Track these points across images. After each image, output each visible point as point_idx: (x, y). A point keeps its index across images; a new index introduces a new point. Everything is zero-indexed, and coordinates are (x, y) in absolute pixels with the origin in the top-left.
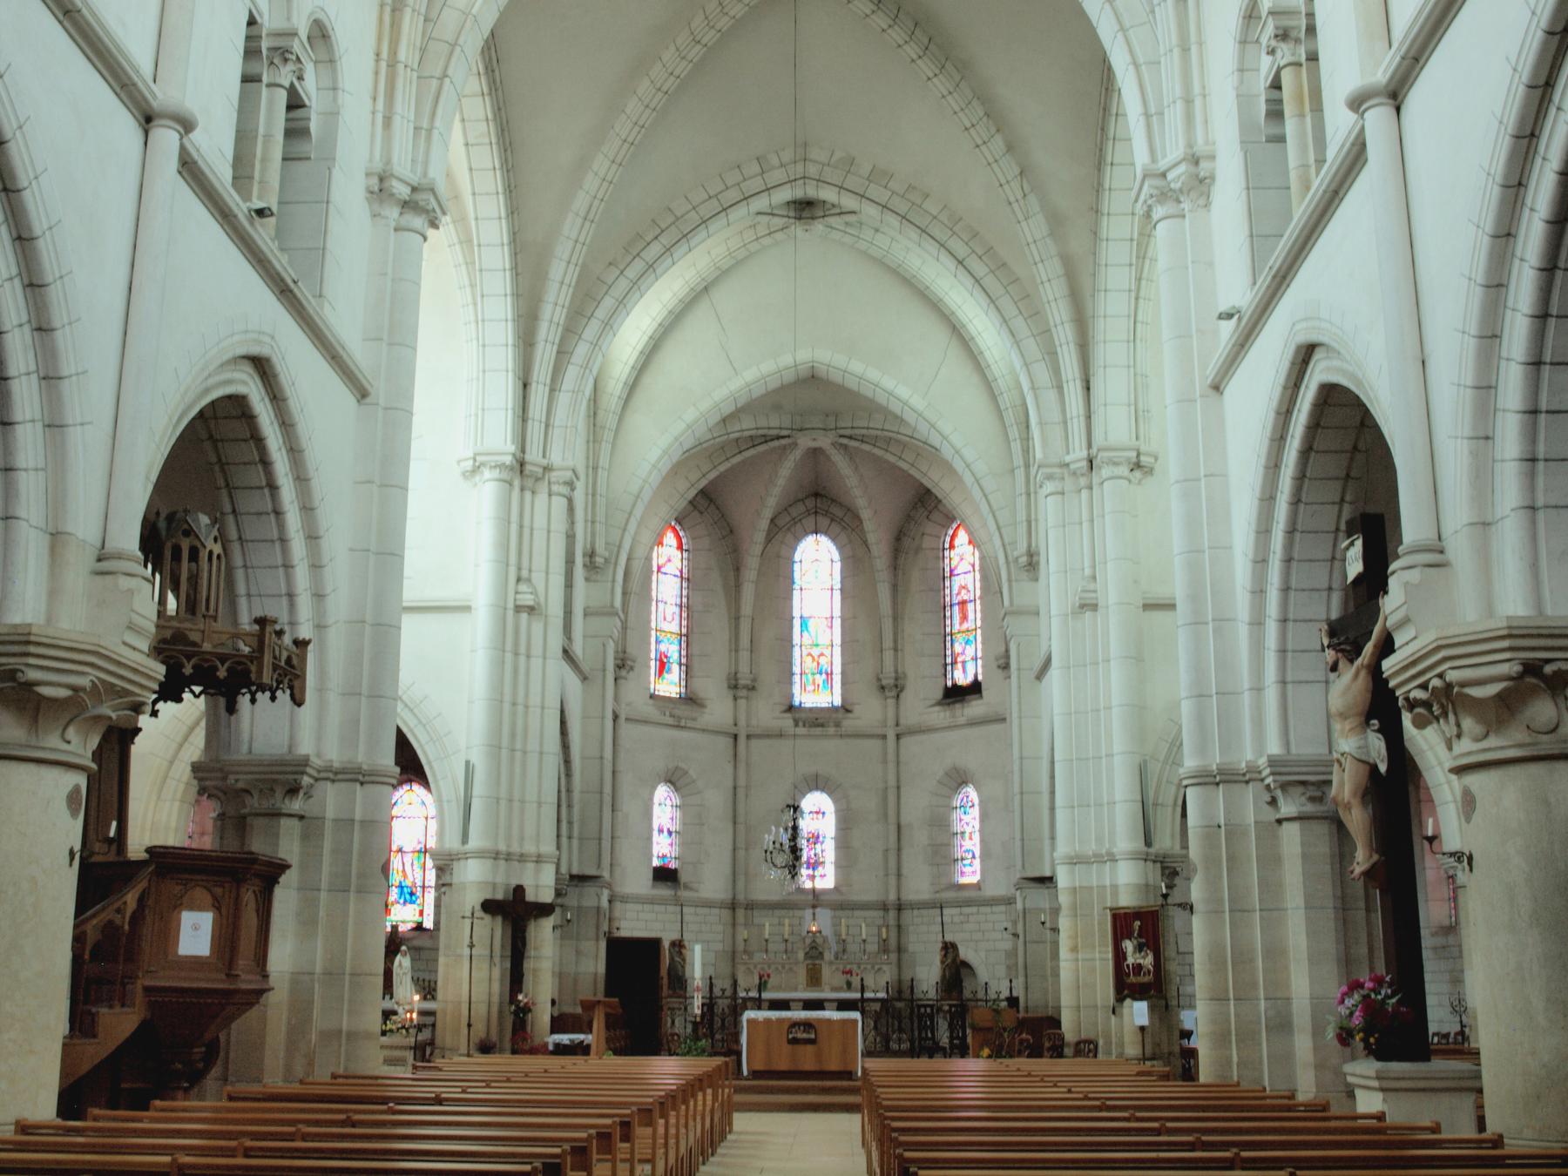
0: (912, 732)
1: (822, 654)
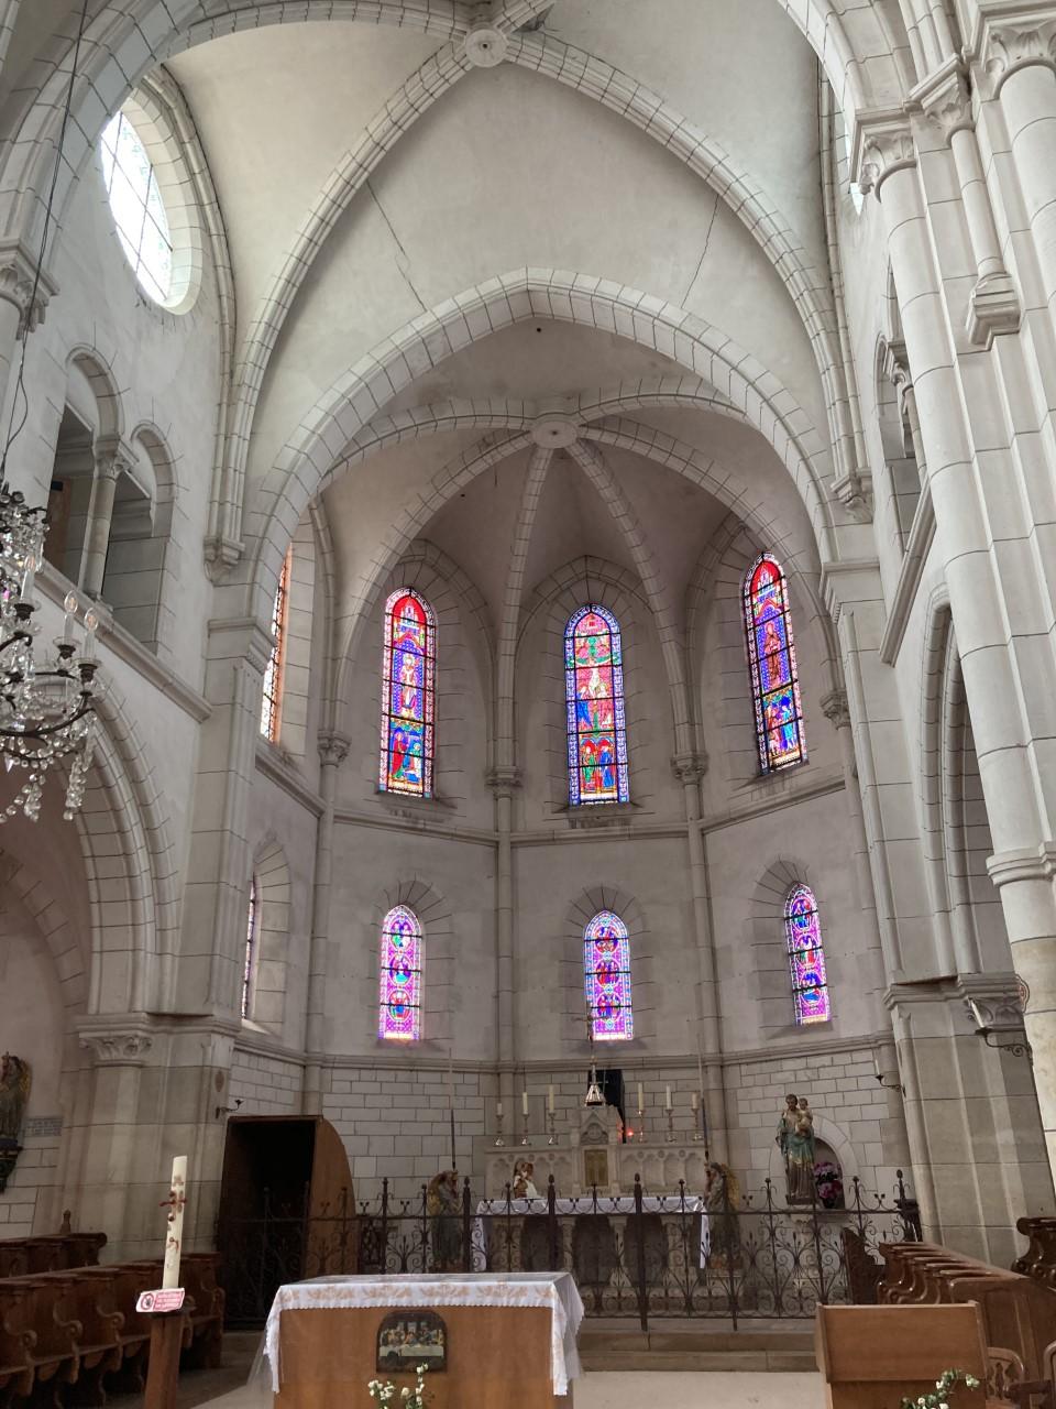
0: (721, 823)
1: (604, 743)
